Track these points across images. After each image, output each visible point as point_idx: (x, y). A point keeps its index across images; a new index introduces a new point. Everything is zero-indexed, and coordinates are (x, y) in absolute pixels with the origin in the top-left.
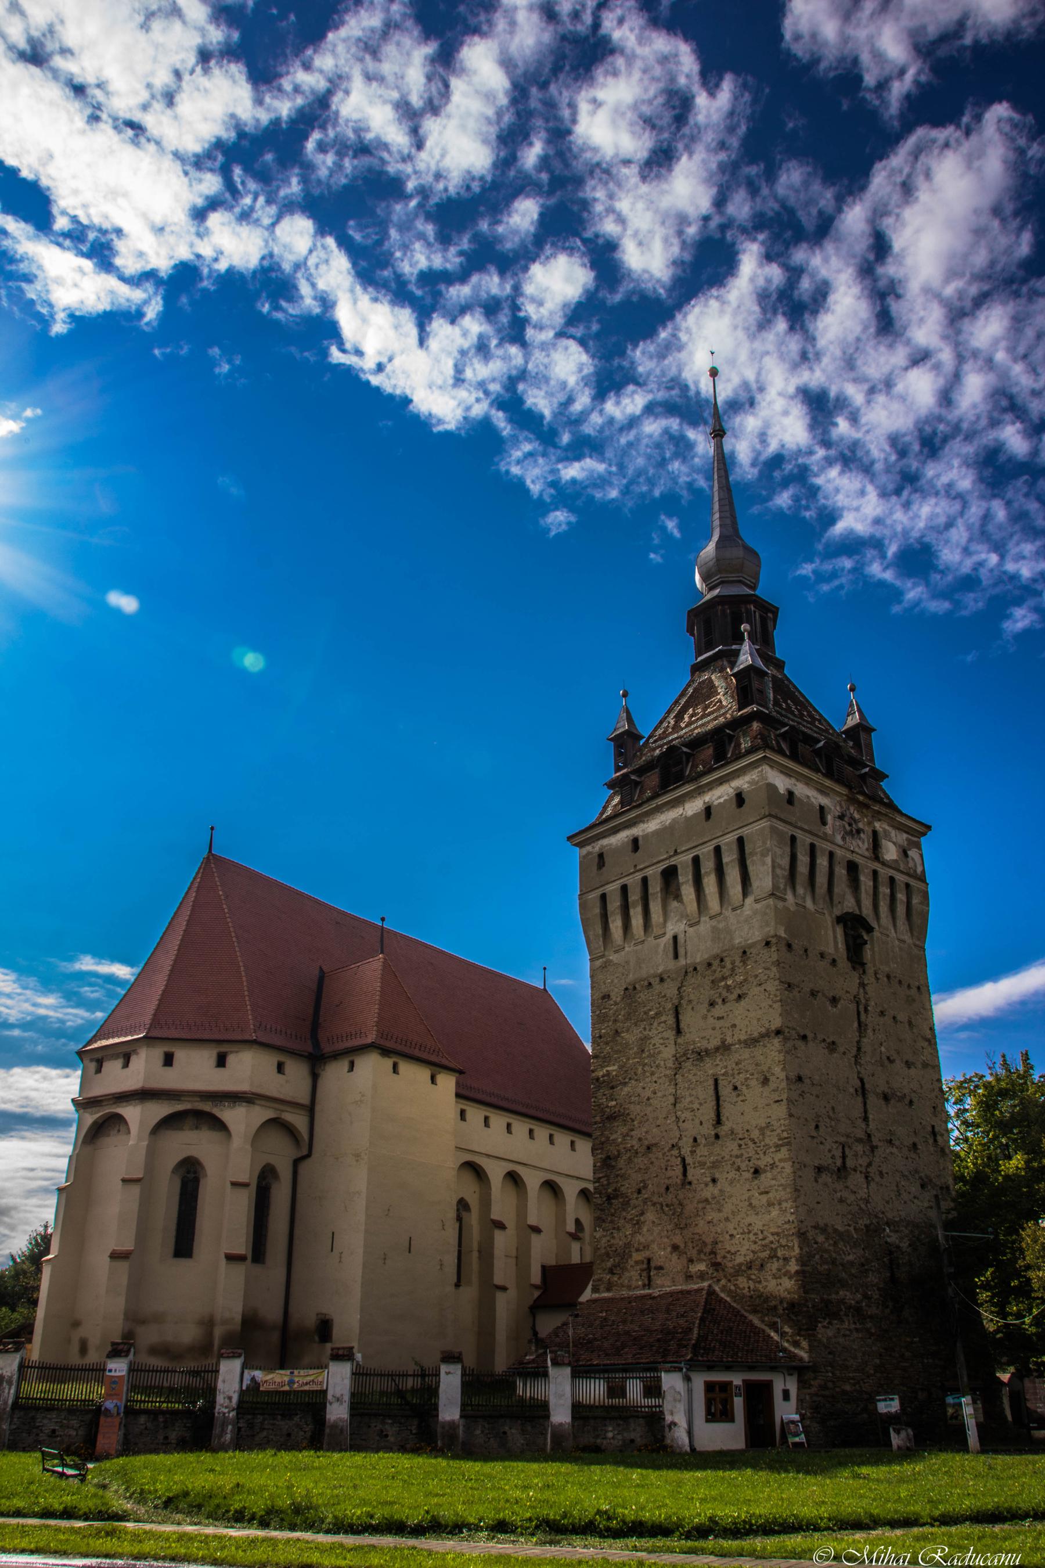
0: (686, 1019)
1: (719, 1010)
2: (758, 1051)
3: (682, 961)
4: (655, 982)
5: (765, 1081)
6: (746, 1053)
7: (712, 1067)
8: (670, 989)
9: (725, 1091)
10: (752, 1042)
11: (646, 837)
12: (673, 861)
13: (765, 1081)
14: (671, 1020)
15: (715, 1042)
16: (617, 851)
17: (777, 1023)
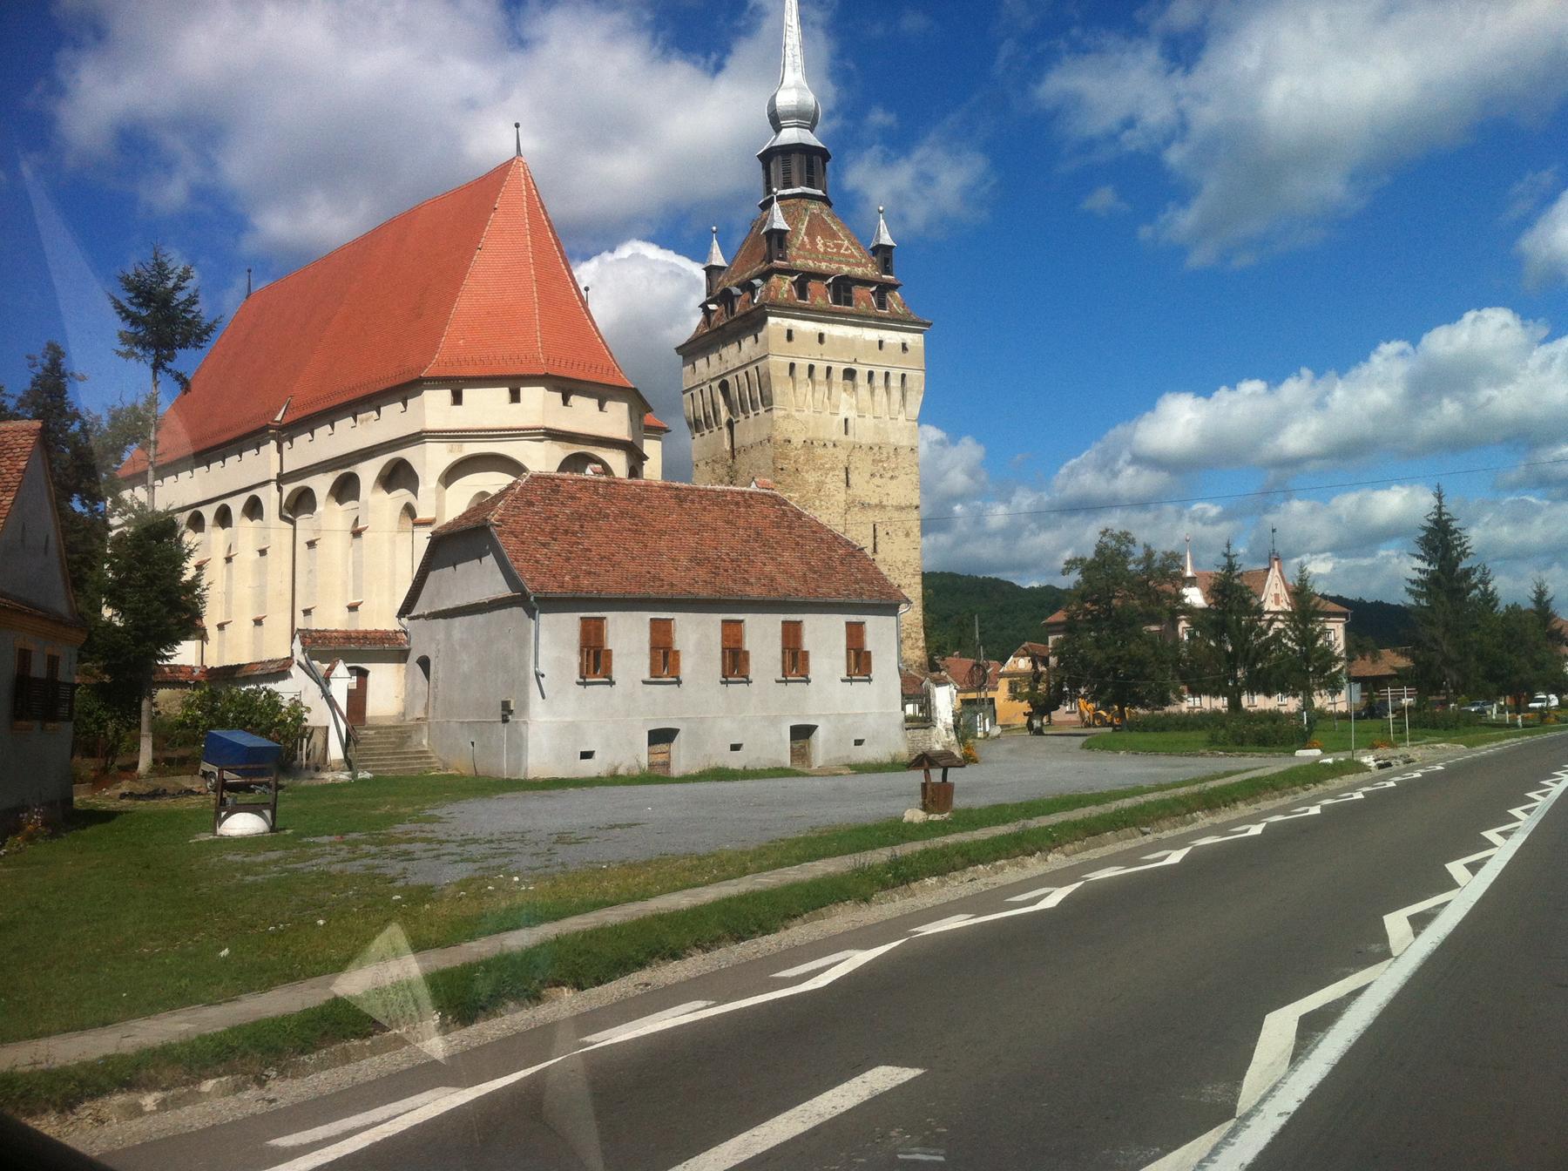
0: (853, 478)
1: (877, 480)
2: (903, 515)
3: (850, 438)
4: (830, 445)
5: (907, 535)
6: (896, 515)
7: (873, 516)
8: (842, 454)
9: (881, 533)
10: (900, 508)
11: (831, 337)
12: (853, 366)
13: (907, 535)
14: (843, 476)
15: (874, 501)
16: (804, 334)
17: (916, 502)
